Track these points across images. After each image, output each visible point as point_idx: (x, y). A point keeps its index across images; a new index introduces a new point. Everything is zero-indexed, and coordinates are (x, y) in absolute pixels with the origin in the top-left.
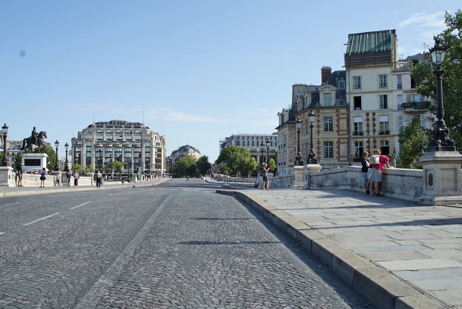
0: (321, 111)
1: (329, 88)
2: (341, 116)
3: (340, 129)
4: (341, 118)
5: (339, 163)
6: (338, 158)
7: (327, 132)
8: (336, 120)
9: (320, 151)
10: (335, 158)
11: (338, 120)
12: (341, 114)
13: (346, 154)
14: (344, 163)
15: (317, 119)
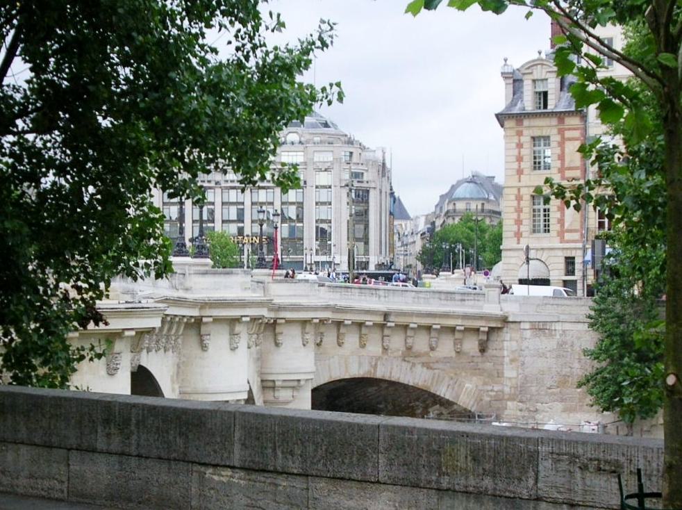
0: (526, 122)
1: (544, 66)
2: (568, 134)
3: (566, 165)
4: (570, 139)
5: (561, 245)
6: (561, 234)
7: (537, 172)
8: (559, 143)
9: (523, 216)
10: (553, 233)
11: (561, 144)
12: (569, 129)
13: (577, 226)
14: (572, 245)
15: (517, 141)
